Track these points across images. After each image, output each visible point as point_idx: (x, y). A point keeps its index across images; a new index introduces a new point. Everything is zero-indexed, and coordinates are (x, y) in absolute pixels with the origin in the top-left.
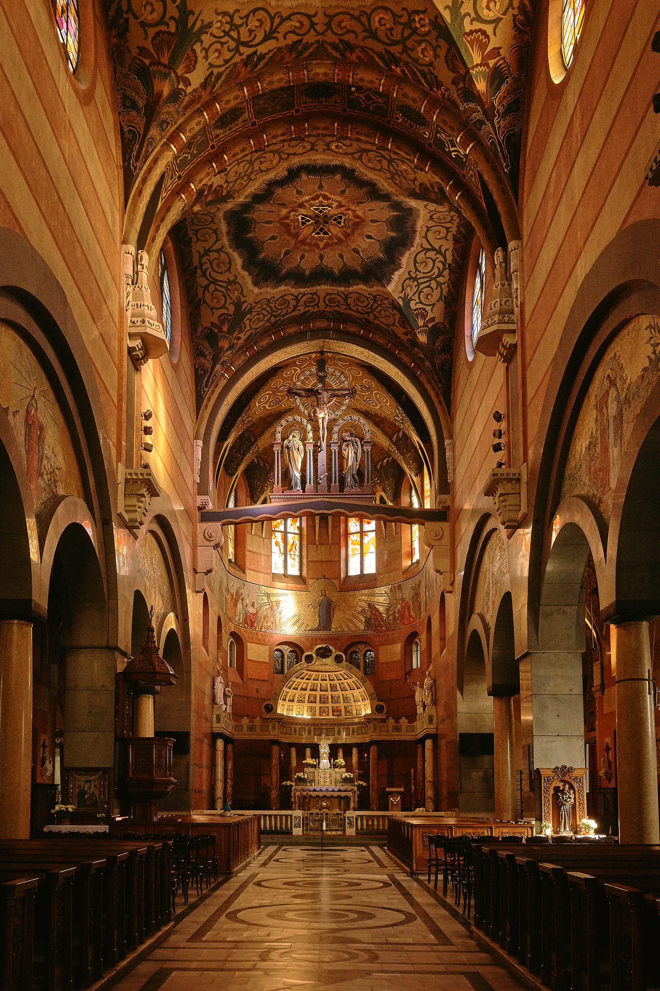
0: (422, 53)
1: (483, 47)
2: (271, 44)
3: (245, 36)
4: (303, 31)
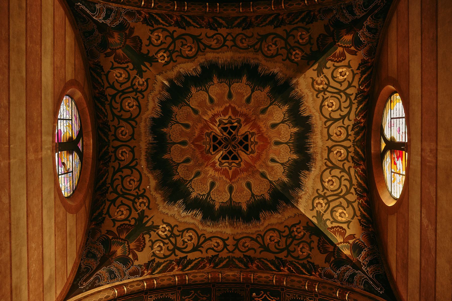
0: (301, 251)
1: (342, 234)
4: (220, 248)
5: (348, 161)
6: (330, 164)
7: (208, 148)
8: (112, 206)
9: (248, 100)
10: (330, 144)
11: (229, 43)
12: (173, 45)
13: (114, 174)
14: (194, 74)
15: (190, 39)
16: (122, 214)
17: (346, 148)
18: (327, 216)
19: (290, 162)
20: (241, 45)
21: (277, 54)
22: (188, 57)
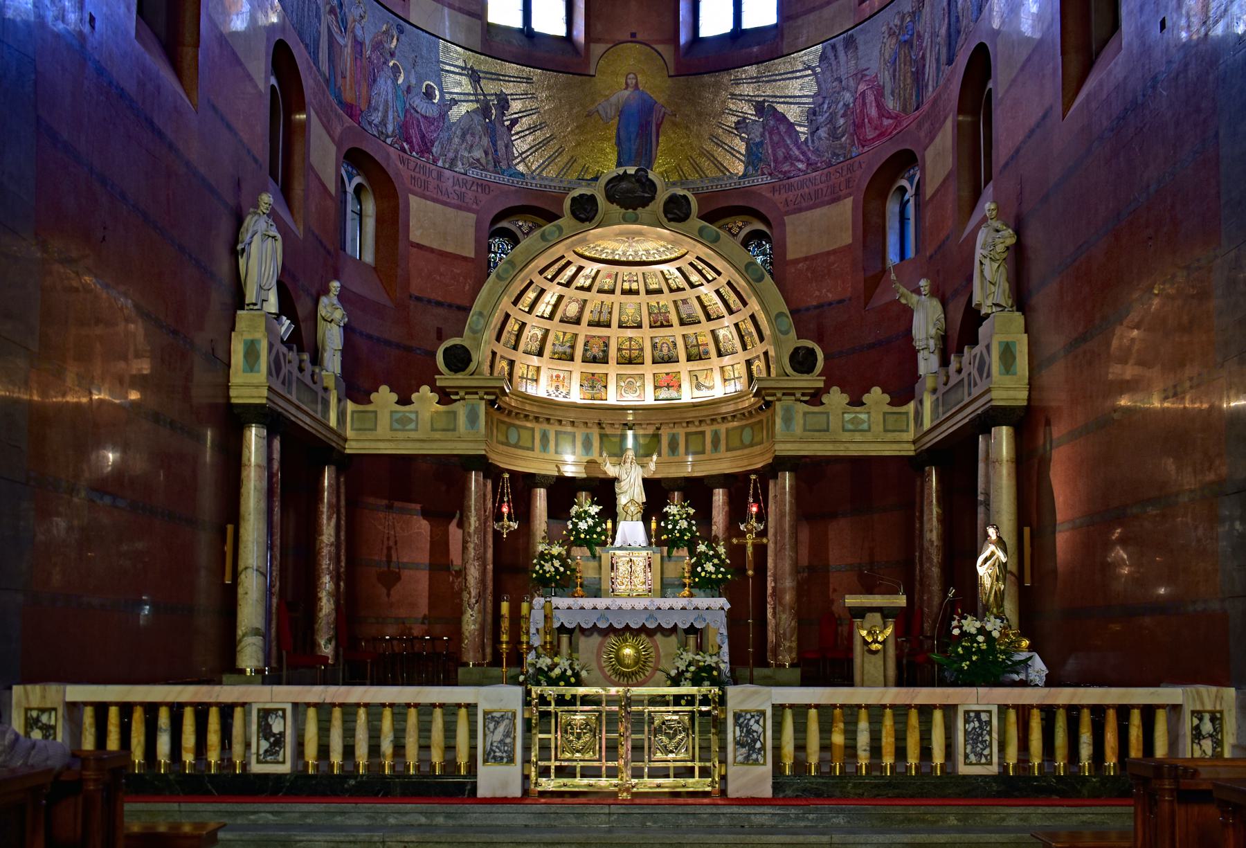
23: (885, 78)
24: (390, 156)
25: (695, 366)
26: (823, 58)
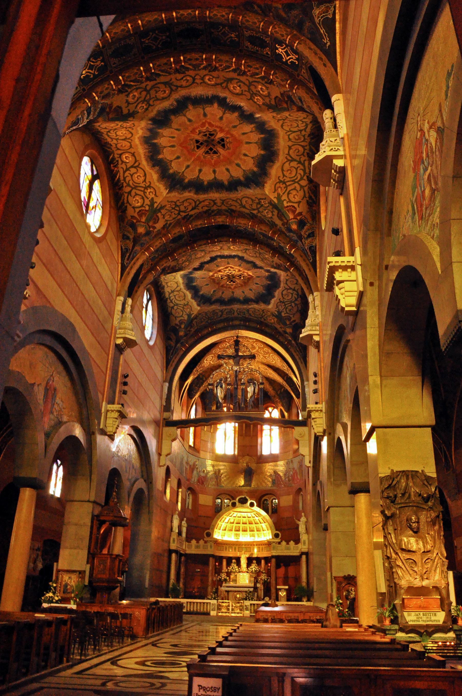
1: (294, 212)
2: (195, 211)
3: (182, 208)
5: (304, 156)
6: (290, 158)
7: (192, 148)
8: (129, 196)
9: (221, 118)
10: (290, 143)
11: (198, 81)
12: (148, 95)
13: (124, 172)
14: (172, 108)
15: (162, 87)
16: (138, 202)
17: (303, 146)
18: (284, 197)
19: (259, 156)
20: (209, 82)
21: (242, 94)
22: (163, 99)
23: (298, 471)
24: (197, 487)
25: (258, 532)
26: (287, 463)
